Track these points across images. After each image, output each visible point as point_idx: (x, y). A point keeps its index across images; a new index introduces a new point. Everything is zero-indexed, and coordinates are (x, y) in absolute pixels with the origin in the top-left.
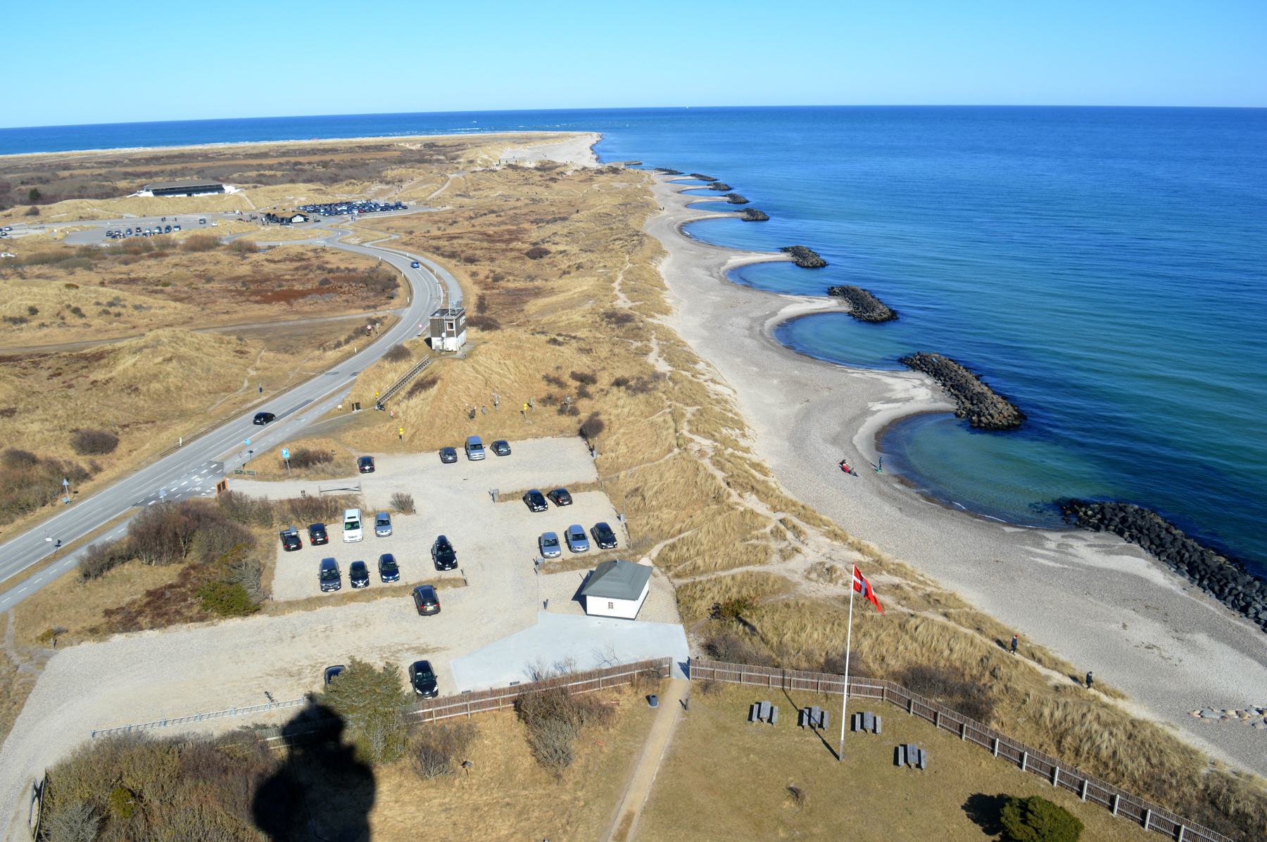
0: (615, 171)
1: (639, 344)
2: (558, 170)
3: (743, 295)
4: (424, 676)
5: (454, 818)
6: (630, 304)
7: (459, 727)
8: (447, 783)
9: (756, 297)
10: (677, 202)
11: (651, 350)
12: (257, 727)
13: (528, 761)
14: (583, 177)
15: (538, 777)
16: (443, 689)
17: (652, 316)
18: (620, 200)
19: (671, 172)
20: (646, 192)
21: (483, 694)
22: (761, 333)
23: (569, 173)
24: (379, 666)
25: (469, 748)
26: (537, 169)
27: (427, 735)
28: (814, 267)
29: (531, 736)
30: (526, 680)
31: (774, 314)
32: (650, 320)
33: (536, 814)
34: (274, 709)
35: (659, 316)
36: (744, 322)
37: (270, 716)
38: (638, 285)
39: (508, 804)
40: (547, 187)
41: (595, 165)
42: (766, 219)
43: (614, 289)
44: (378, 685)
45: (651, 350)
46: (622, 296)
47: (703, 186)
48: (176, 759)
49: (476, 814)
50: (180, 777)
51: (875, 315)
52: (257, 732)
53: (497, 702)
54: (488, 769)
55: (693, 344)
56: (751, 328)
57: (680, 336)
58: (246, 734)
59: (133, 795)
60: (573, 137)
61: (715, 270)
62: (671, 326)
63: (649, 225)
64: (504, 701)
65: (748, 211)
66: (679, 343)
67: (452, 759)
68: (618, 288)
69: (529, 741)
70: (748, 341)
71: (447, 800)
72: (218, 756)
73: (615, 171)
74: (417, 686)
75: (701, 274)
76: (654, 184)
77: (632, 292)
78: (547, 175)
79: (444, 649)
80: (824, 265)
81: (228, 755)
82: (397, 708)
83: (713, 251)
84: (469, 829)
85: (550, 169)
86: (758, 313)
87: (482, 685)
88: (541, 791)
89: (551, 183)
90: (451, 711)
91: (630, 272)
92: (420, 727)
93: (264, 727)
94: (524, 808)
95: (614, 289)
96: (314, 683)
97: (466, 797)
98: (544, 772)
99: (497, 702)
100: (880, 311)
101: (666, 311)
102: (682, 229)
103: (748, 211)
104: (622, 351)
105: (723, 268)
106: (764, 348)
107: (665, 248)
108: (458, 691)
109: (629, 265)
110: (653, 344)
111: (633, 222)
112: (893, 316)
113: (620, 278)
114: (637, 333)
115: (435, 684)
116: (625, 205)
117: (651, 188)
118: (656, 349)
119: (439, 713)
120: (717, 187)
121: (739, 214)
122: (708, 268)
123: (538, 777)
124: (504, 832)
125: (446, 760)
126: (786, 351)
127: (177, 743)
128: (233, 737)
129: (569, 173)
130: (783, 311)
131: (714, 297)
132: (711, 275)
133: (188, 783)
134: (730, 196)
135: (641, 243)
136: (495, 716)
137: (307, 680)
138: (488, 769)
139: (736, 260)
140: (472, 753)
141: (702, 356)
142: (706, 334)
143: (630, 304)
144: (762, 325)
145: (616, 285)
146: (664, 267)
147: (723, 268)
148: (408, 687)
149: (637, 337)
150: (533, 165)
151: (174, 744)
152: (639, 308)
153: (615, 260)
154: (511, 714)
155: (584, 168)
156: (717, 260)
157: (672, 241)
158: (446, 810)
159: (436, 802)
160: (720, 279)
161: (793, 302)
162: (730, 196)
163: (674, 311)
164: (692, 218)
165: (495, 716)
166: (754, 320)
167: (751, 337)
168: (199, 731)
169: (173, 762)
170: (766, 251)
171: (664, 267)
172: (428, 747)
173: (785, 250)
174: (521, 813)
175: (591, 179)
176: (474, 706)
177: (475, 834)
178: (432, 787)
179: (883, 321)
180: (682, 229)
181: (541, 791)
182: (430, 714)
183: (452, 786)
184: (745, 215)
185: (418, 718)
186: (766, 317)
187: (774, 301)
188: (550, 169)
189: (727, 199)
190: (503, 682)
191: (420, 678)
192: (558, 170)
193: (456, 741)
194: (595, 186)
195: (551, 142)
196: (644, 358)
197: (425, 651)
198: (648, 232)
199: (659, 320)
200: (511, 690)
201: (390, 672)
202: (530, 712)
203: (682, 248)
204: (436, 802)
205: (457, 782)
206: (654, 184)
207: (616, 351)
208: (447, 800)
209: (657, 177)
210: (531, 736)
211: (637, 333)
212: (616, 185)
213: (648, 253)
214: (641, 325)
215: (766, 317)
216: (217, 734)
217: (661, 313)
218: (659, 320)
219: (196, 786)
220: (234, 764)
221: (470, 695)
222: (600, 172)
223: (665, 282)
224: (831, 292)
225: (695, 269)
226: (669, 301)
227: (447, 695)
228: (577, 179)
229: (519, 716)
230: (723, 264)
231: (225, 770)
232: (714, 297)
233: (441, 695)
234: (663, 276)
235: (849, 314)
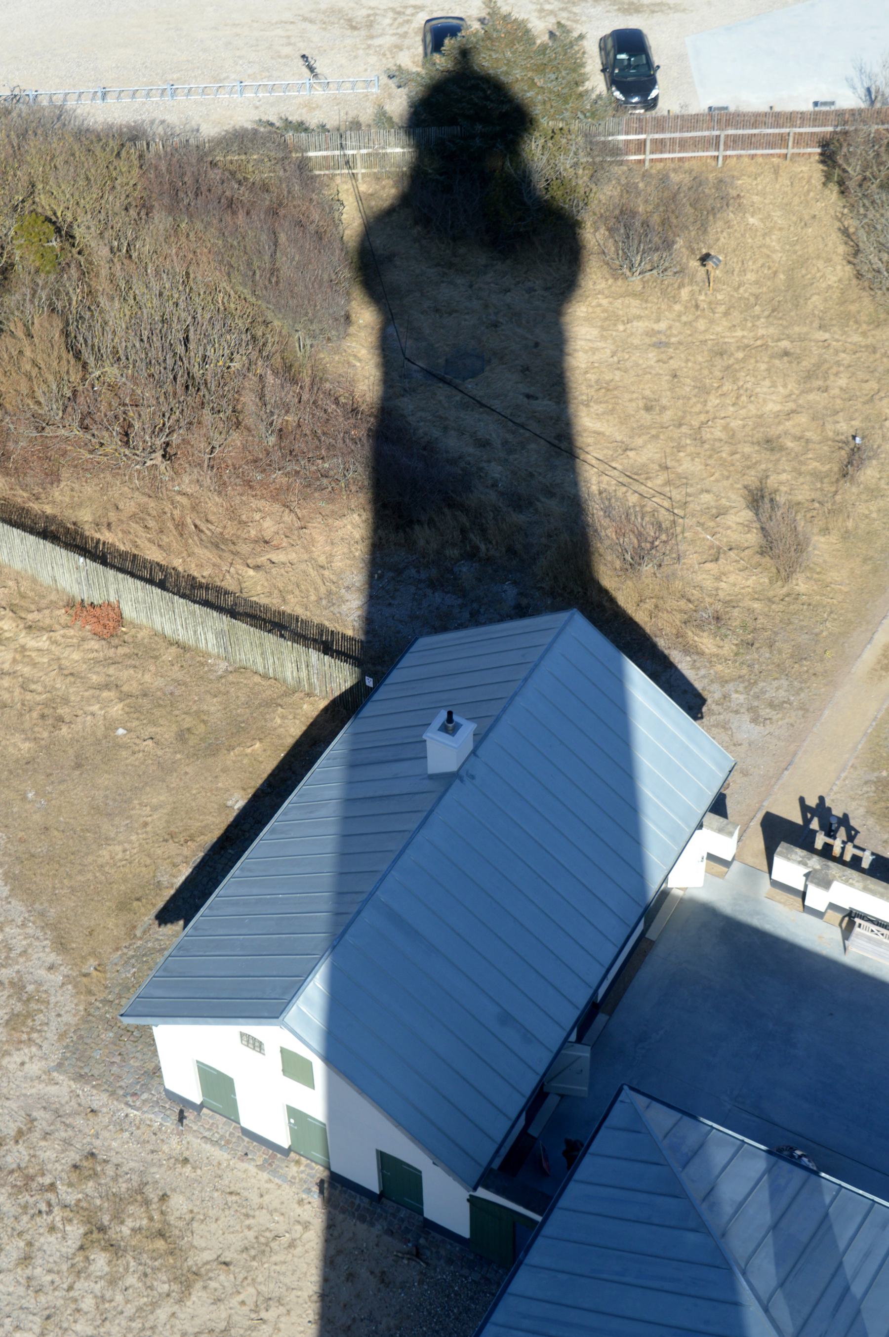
4: (631, 63)
5: (674, 364)
7: (698, 182)
8: (664, 292)
12: (288, 124)
13: (837, 273)
15: (853, 308)
16: (669, 96)
21: (756, 119)
24: (540, 27)
25: (716, 227)
27: (629, 189)
29: (852, 224)
30: (849, 99)
33: (842, 382)
34: (319, 93)
37: (310, 106)
39: (786, 353)
44: (541, 69)
48: (136, 171)
49: (719, 363)
50: (146, 208)
52: (289, 135)
53: (782, 140)
54: (750, 277)
58: (266, 139)
59: (58, 230)
64: (799, 140)
67: (680, 243)
69: (845, 232)
71: (662, 326)
72: (215, 175)
74: (614, 81)
79: (676, 9)
81: (233, 174)
82: (575, 126)
84: (703, 390)
87: (753, 99)
88: (856, 338)
90: (683, 145)
92: (616, 169)
93: (301, 127)
94: (818, 366)
96: (400, 48)
97: (701, 325)
98: (866, 301)
99: (782, 140)
108: (700, 105)
115: (652, 83)
119: (659, 146)
123: (853, 308)
124: (772, 407)
125: (668, 245)
127: (134, 139)
128: (241, 139)
133: (161, 221)
136: (776, 171)
137: (387, 41)
138: (750, 277)
140: (721, 238)
148: (596, 83)
151: (131, 138)
154: (810, 168)
158: (659, 345)
159: (640, 326)
165: (776, 171)
168: (172, 118)
169: (128, 175)
172: (634, 214)
174: (809, 376)
176: (735, 142)
177: (713, 401)
178: (634, 295)
181: (856, 338)
182: (640, 147)
183: (675, 299)
185: (615, 151)
190: (799, 98)
191: (626, 67)
193: (689, 210)
197: (636, 9)
200: (815, 117)
201: (562, 41)
202: (854, 170)
204: (640, 326)
205: (685, 293)
208: (662, 326)
210: (852, 224)
216: (210, 130)
219: (176, 228)
220: (244, 194)
221: (719, 117)
227: (676, 110)
229: (828, 177)
231: (231, 204)
233: (663, 107)
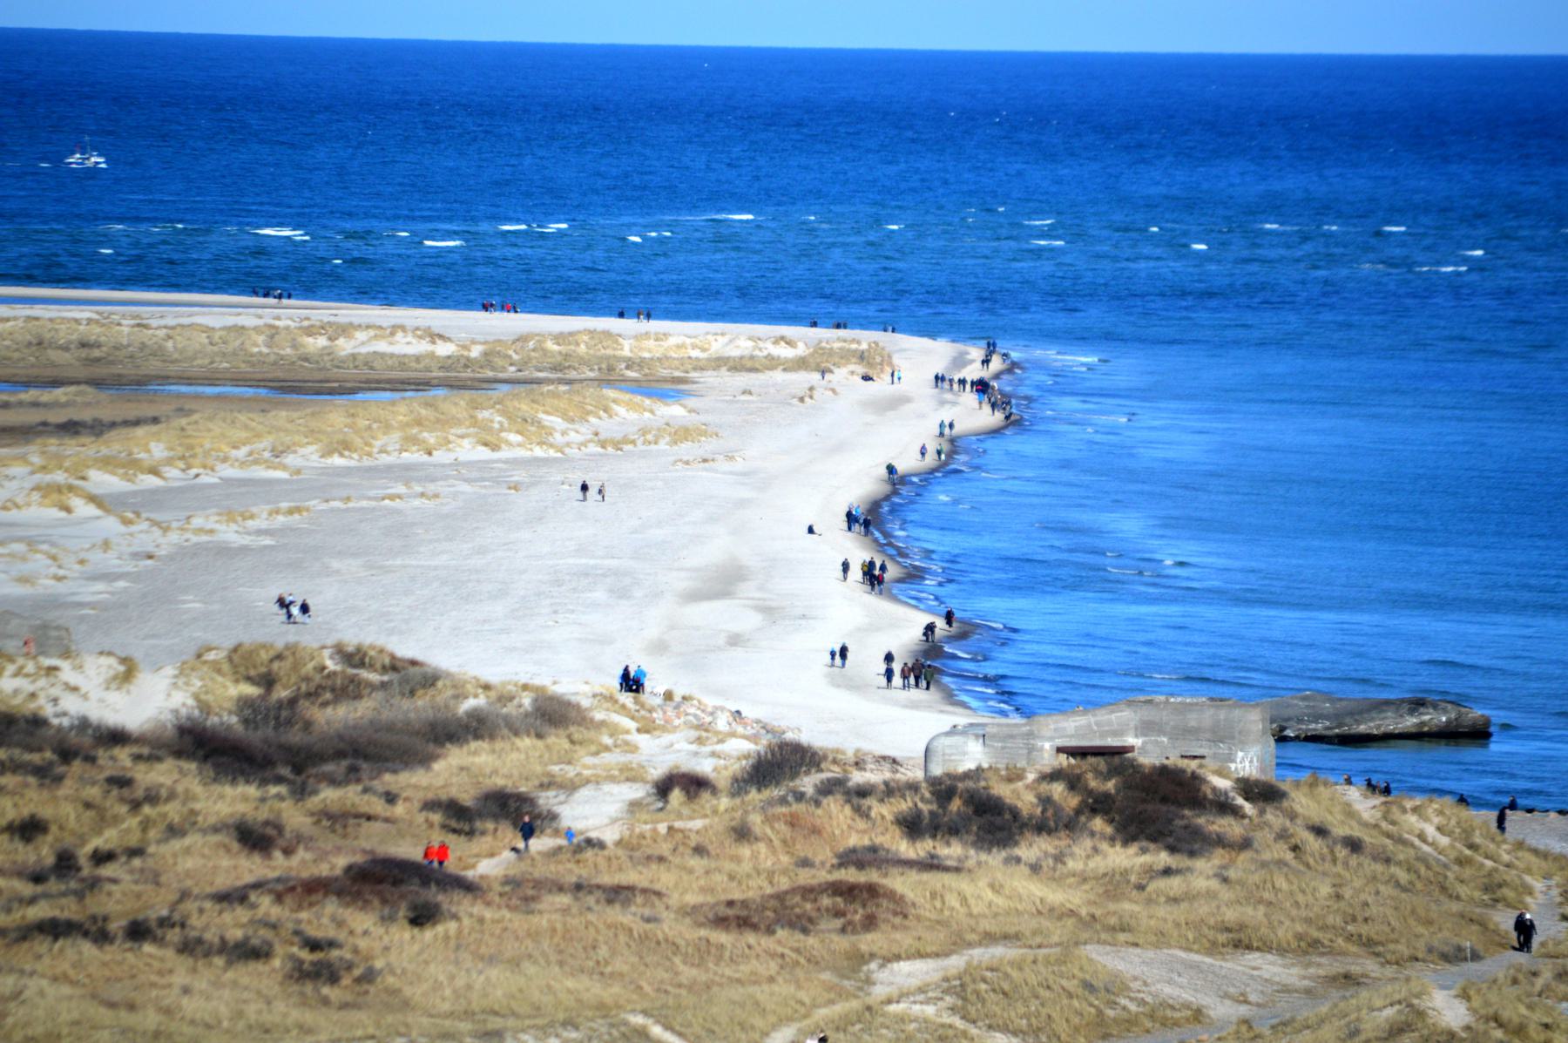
2: (460, 770)
14: (761, 868)
23: (595, 812)
26: (198, 743)
40: (319, 968)
41: (917, 733)
60: (658, 383)
73: (1154, 805)
78: (328, 828)
85: (366, 754)
89: (365, 930)
129: (595, 812)
150: (153, 702)
155: (780, 763)
175: (856, 898)
188: (366, 754)
192: (460, 770)
194: (906, 980)
195: (386, 434)
222: (970, 813)
228: (687, 885)
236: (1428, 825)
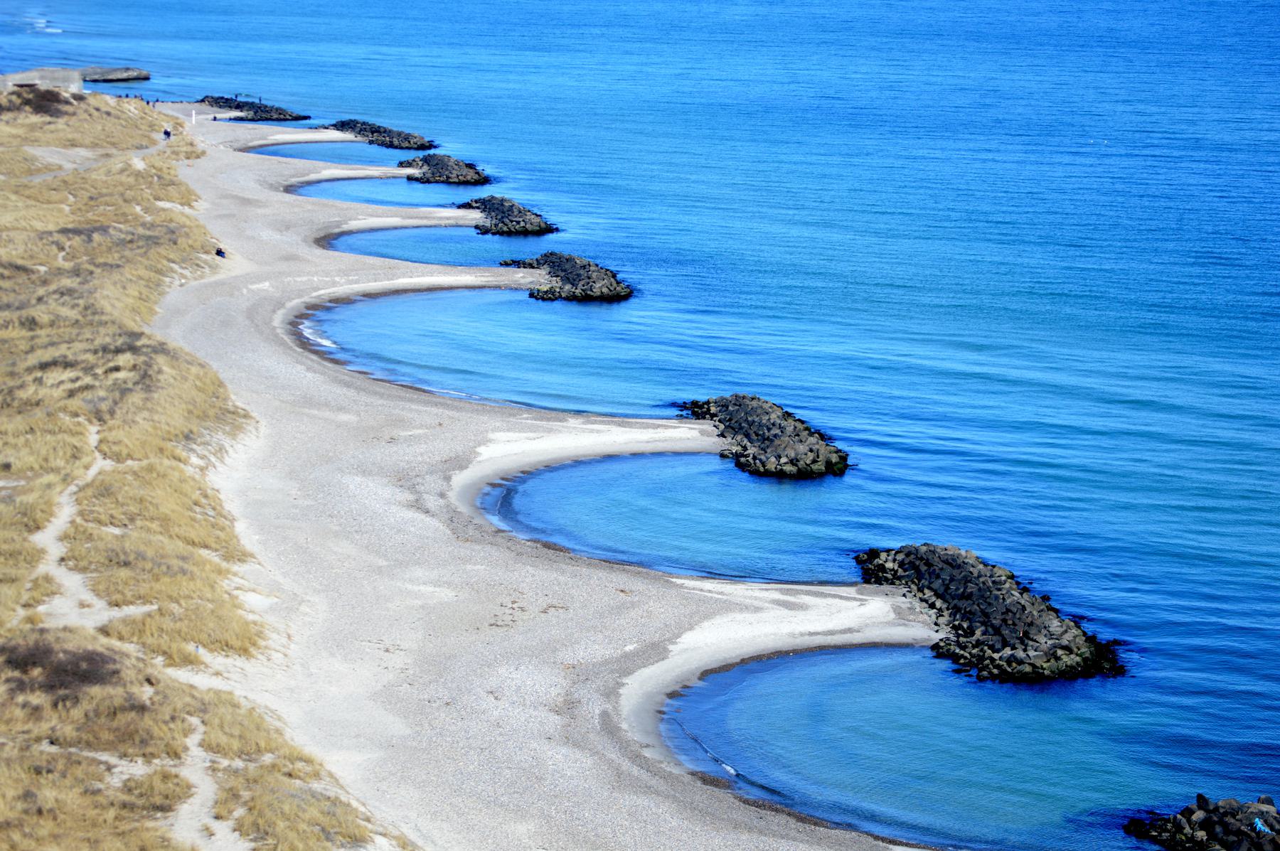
0: (45, 102)
1: (138, 769)
3: (537, 578)
6: (101, 613)
9: (594, 587)
10: (286, 227)
11: (186, 791)
17: (189, 661)
18: (63, 213)
19: (262, 113)
20: (164, 183)
22: (609, 726)
28: (804, 476)
31: (655, 651)
32: (182, 675)
35: (216, 660)
36: (545, 683)
38: (134, 538)
42: (618, 296)
43: (36, 555)
45: (186, 791)
46: (72, 582)
47: (387, 165)
51: (1033, 655)
55: (347, 769)
56: (568, 707)
57: (300, 738)
61: (432, 483)
62: (263, 699)
63: (177, 311)
65: (554, 262)
66: (296, 765)
68: (57, 551)
70: (559, 757)
73: (45, 102)
75: (377, 496)
76: (194, 154)
77: (112, 567)
80: (838, 468)
83: (420, 413)
86: (594, 650)
91: (103, 490)
95: (36, 555)
100: (1053, 641)
101: (243, 643)
102: (311, 327)
103: (554, 262)
104: (73, 798)
105: (461, 479)
106: (620, 780)
107: (238, 399)
109: (101, 464)
110: (194, 768)
111: (114, 298)
112: (1104, 662)
113: (65, 513)
114: (131, 728)
116: (85, 232)
117: (184, 171)
118: (206, 789)
120: (438, 172)
121: (522, 277)
122: (404, 479)
126: (703, 794)
130: (689, 639)
131: (427, 588)
132: (418, 505)
134: (486, 205)
135: (146, 379)
139: (511, 446)
141: (385, 813)
142: (397, 727)
143: (101, 613)
144: (611, 693)
145: (48, 539)
146: (235, 473)
147: (461, 479)
149: (132, 741)
152: (137, 629)
153: (43, 443)
156: (442, 448)
157: (265, 374)
160: (452, 518)
161: (728, 607)
162: (486, 205)
163: (274, 640)
164: (344, 288)
166: (580, 674)
167: (570, 740)
170: (619, 416)
171: (235, 473)
173: (696, 410)
179: (1067, 677)
180: (311, 327)
184: (541, 279)
186: (627, 665)
187: (654, 602)
189: (476, 216)
196: (157, 825)
198: (175, 337)
199: (215, 675)
203: (309, 401)
206: (194, 154)
207: (48, 795)
209: (211, 132)
211: (131, 728)
212: (46, 154)
213: (173, 417)
214: (146, 693)
215: (627, 665)
217: (225, 647)
218: (215, 675)
223: (241, 527)
224: (870, 570)
225: (354, 482)
226: (255, 603)
230: (461, 463)
232: (427, 588)
234: (232, 506)
235: (938, 651)
236: (132, 107)
